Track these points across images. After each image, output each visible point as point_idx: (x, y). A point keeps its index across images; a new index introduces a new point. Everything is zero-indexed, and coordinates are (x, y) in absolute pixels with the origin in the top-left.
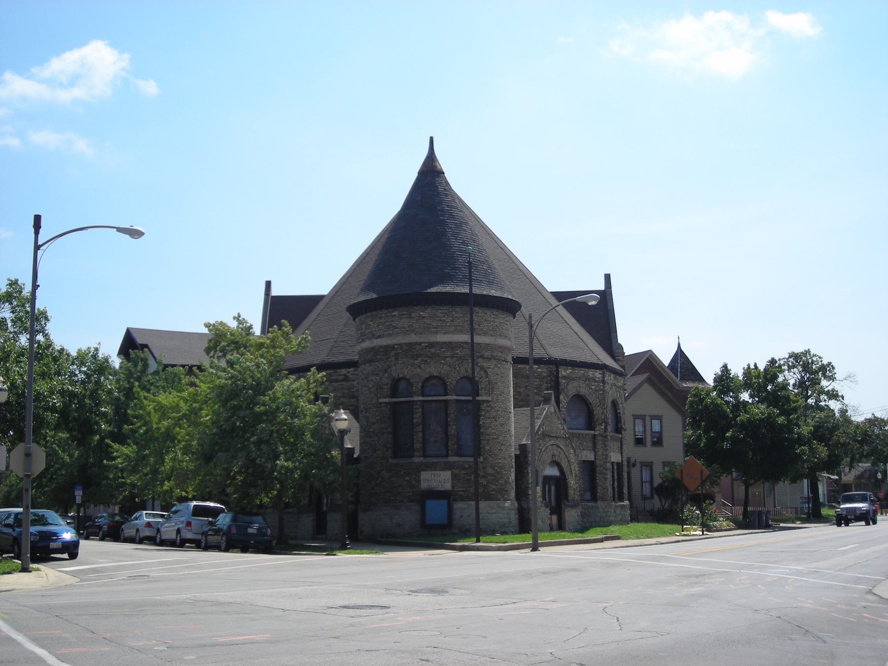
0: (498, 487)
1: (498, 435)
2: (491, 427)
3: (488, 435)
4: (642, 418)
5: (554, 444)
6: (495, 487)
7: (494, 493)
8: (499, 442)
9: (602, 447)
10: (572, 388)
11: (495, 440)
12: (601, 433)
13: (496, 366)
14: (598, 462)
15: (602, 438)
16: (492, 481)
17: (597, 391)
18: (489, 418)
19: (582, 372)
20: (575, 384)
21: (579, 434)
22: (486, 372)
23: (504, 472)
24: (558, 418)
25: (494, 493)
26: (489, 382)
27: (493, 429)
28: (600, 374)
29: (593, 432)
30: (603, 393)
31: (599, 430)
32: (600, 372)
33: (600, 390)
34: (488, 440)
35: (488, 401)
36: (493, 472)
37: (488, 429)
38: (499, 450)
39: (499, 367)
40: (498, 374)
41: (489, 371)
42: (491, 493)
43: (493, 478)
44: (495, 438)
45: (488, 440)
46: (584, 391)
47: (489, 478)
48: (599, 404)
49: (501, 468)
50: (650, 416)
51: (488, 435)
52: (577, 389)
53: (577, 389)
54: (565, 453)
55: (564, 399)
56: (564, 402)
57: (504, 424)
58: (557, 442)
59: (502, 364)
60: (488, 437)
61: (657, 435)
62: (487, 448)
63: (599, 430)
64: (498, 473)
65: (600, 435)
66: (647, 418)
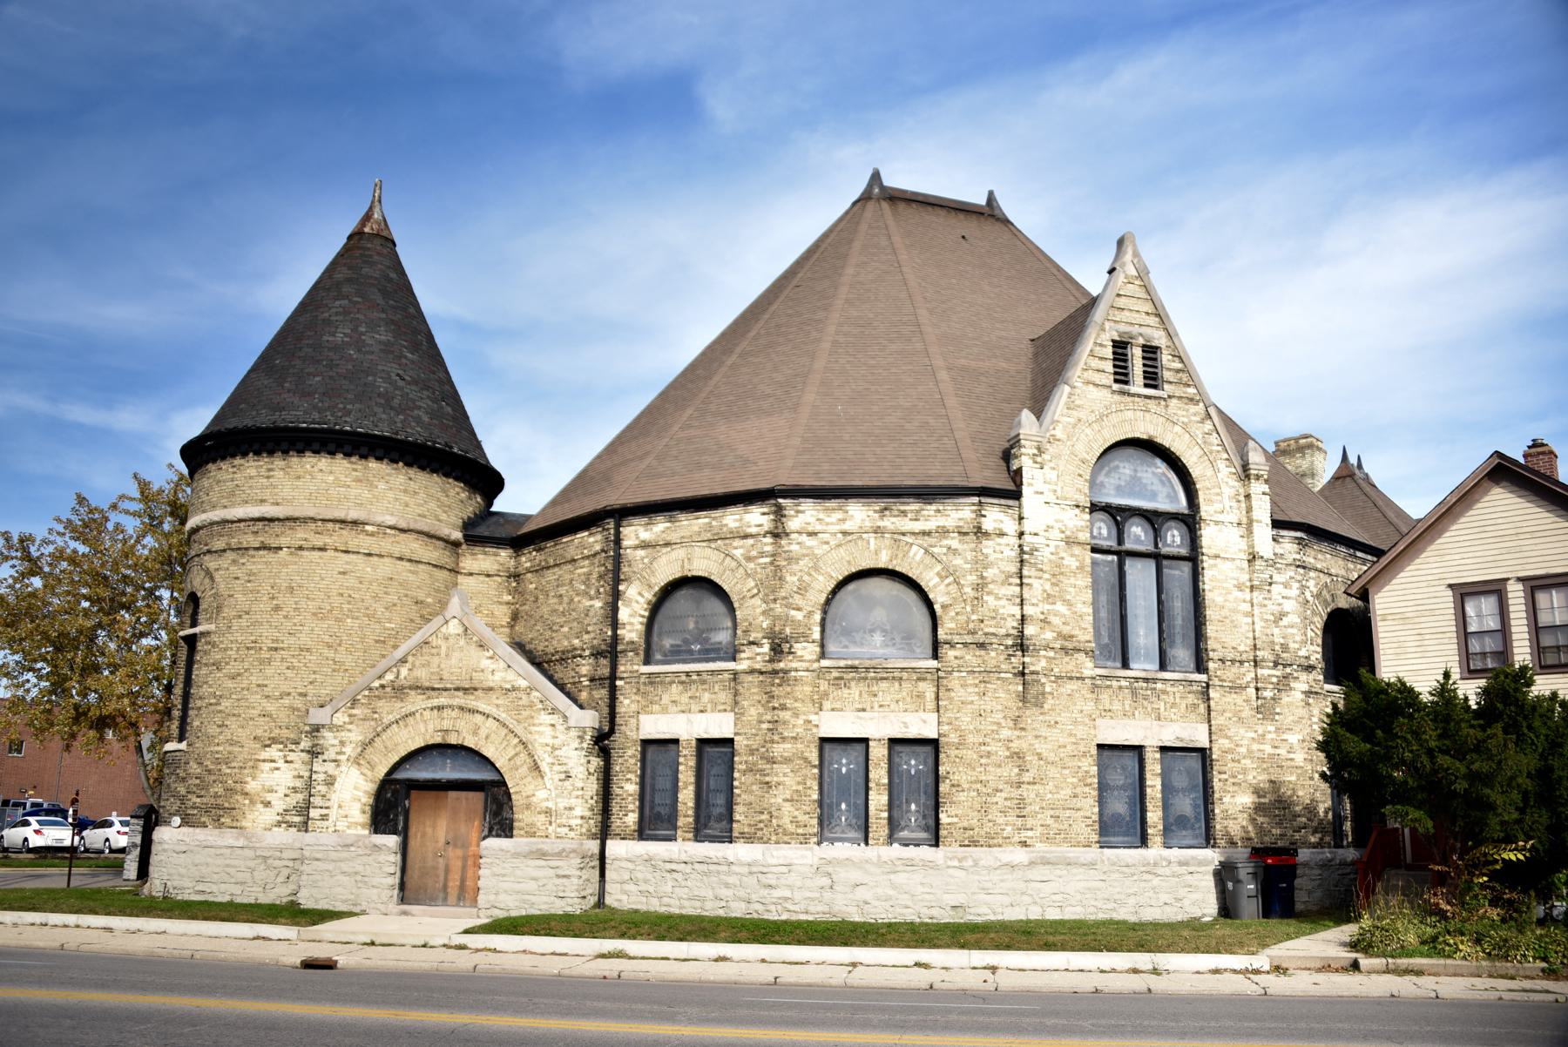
0: (205, 800)
1: (221, 697)
2: (206, 683)
3: (200, 698)
4: (1495, 589)
5: (451, 707)
6: (198, 800)
7: (195, 812)
8: (220, 711)
9: (760, 702)
10: (667, 569)
11: (213, 708)
12: (757, 666)
13: (234, 561)
14: (740, 743)
15: (761, 678)
16: (195, 789)
17: (749, 559)
18: (206, 665)
19: (700, 521)
20: (680, 553)
21: (688, 674)
22: (212, 578)
23: (228, 771)
24: (481, 646)
25: (195, 812)
26: (216, 595)
27: (210, 686)
28: (764, 514)
29: (731, 665)
30: (772, 563)
31: (748, 658)
32: (765, 510)
33: (762, 554)
34: (200, 708)
35: (208, 633)
36: (199, 771)
37: (201, 687)
38: (219, 726)
39: (243, 564)
40: (237, 578)
41: (217, 576)
42: (189, 812)
43: (198, 781)
44: (211, 704)
45: (200, 708)
46: (703, 563)
47: (190, 782)
48: (755, 591)
49: (217, 762)
50: (1519, 579)
51: (200, 698)
52: (683, 567)
53: (683, 567)
54: (504, 725)
55: (640, 594)
56: (637, 602)
57: (239, 675)
58: (456, 702)
59: (253, 556)
60: (199, 703)
61: (1490, 644)
62: (196, 723)
63: (748, 658)
64: (209, 772)
65: (752, 671)
66: (1509, 588)
